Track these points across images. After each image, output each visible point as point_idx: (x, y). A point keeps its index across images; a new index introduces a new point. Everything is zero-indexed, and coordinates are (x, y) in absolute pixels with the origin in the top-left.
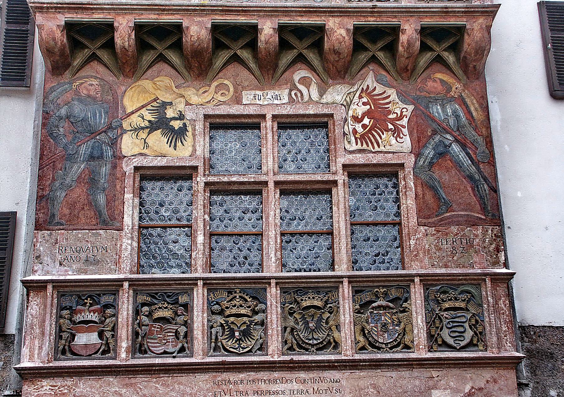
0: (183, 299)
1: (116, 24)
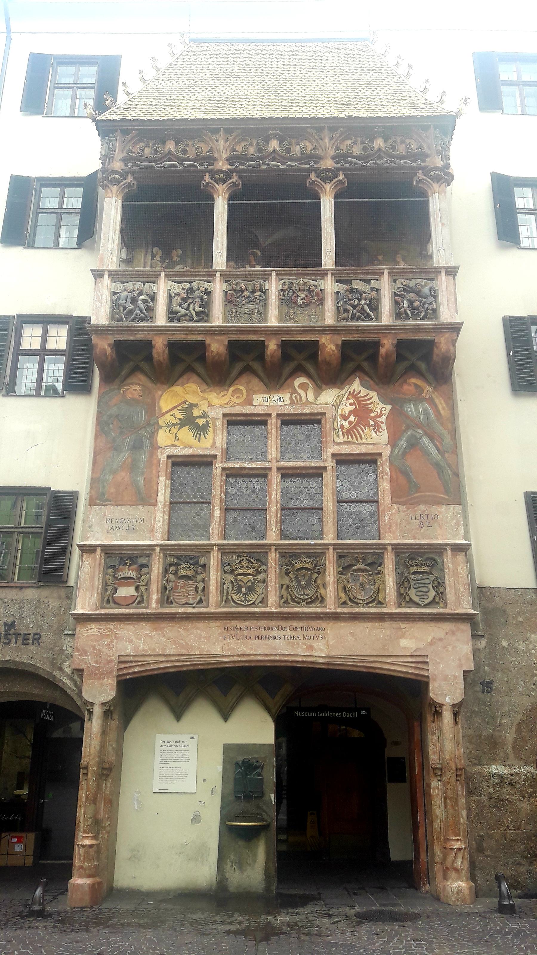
0: (202, 561)
1: (153, 343)
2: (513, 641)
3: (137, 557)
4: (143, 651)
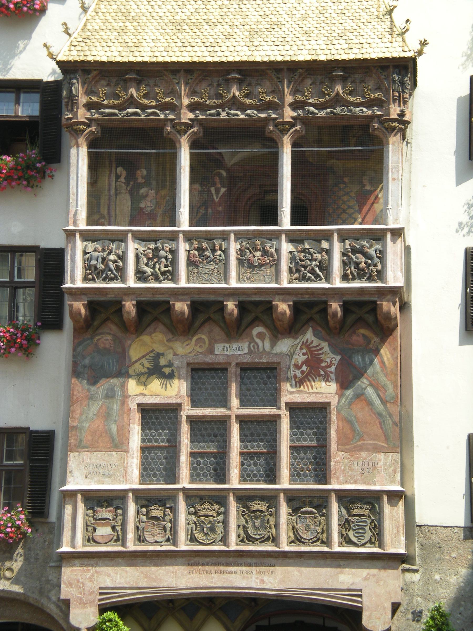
2: (446, 575)
3: (112, 500)
4: (120, 583)
